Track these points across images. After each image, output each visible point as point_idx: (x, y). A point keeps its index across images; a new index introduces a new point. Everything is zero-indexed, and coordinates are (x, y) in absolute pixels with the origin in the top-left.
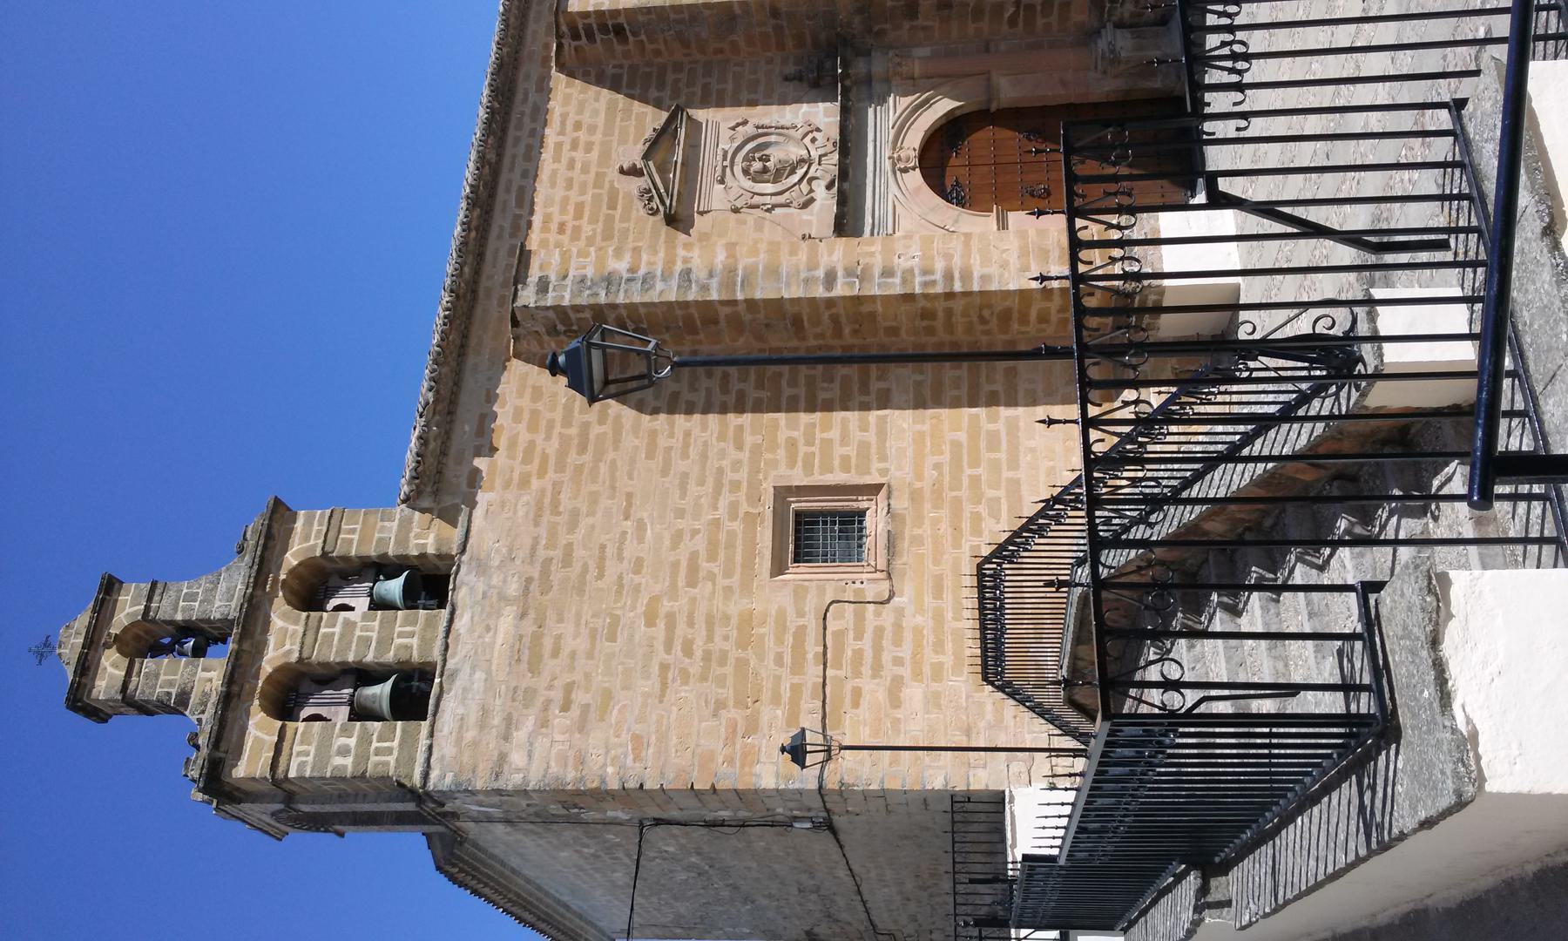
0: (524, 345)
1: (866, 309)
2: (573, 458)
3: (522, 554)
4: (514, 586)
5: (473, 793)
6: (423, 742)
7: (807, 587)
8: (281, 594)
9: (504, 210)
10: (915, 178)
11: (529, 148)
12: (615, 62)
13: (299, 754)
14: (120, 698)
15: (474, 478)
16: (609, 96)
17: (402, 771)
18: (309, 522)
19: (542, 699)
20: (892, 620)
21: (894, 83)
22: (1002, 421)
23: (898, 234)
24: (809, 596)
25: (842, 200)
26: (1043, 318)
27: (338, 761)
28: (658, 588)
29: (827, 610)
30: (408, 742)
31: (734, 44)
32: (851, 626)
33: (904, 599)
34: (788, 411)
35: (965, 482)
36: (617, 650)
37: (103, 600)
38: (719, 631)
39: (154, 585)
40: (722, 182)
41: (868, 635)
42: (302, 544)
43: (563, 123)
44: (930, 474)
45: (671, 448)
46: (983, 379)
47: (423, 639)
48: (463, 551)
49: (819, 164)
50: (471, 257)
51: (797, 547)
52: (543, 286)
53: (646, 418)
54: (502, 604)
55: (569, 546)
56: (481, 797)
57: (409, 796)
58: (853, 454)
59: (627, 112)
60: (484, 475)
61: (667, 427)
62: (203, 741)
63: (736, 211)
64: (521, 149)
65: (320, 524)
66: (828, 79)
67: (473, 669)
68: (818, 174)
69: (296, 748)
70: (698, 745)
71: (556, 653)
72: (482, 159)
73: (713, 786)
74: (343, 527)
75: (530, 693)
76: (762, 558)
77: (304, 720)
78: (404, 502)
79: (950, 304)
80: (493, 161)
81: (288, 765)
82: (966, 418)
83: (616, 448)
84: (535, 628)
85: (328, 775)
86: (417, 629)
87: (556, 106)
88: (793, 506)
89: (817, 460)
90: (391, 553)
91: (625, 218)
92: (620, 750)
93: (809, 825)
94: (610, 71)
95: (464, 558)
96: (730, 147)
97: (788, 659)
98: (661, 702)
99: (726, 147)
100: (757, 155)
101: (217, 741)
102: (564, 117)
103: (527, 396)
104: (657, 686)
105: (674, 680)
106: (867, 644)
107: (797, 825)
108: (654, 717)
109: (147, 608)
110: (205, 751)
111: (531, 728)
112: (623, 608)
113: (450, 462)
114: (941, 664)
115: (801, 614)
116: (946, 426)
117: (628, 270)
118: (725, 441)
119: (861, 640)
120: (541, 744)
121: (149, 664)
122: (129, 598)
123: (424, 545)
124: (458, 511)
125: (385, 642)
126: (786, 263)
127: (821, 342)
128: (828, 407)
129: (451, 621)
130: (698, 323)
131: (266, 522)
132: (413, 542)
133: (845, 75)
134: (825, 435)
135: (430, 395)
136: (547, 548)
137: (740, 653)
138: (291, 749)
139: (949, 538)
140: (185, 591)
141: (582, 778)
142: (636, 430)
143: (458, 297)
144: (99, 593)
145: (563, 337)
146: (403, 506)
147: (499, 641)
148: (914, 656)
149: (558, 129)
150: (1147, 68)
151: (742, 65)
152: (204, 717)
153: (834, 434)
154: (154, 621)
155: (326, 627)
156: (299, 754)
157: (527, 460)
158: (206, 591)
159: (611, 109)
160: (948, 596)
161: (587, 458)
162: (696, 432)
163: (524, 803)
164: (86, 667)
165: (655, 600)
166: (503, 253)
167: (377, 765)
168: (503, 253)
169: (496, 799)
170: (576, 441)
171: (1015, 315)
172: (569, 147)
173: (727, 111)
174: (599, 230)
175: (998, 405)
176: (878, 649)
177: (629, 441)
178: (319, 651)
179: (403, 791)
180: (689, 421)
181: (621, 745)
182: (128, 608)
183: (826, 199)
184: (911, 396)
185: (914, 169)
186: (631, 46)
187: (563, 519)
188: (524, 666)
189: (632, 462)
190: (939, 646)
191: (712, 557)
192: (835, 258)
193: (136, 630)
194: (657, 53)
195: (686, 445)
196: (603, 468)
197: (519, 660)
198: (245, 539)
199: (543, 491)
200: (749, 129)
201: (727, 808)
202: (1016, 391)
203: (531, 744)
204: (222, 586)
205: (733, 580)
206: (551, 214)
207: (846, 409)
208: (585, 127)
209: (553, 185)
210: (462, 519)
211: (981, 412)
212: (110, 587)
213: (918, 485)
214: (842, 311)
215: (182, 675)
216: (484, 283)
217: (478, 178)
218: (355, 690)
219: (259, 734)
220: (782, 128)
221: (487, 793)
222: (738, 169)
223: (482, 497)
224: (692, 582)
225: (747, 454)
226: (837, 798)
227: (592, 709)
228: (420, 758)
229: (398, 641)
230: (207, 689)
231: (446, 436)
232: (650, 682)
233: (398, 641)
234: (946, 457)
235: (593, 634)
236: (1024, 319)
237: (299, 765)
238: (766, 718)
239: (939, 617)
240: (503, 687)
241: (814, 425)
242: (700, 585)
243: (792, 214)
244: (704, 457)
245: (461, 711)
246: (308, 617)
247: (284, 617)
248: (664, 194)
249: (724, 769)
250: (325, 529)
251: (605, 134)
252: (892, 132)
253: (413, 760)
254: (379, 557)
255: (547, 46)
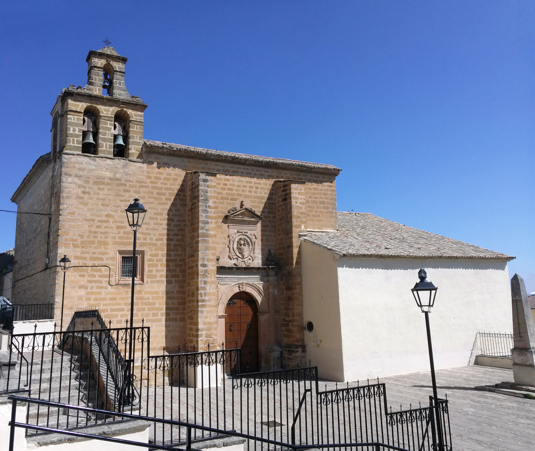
0: (189, 175)
1: (195, 276)
2: (155, 191)
3: (128, 178)
4: (119, 176)
5: (61, 167)
6: (75, 153)
7: (114, 261)
8: (120, 109)
9: (231, 167)
10: (237, 290)
11: (251, 174)
12: (277, 198)
13: (74, 118)
14: (92, 66)
15: (150, 163)
16: (266, 197)
17: (68, 147)
18: (140, 116)
19: (86, 185)
20: (104, 286)
21: (267, 283)
22: (161, 317)
23: (219, 285)
24: (112, 261)
25: (230, 268)
26: (191, 329)
27: (72, 129)
28: (116, 217)
29: (107, 267)
30: (76, 148)
31: (280, 235)
32: (103, 274)
33: (110, 289)
34: (167, 254)
35: (143, 307)
36: (99, 206)
37: (120, 59)
38: (103, 236)
39: (124, 73)
40: (238, 232)
41: (100, 279)
42: (133, 114)
43: (258, 183)
44: (146, 296)
45: (157, 219)
46: (174, 311)
47: (105, 151)
48: (130, 161)
49: (242, 261)
50: (217, 158)
51: (127, 257)
52: (205, 181)
53: (167, 212)
54: (114, 173)
55: (129, 191)
56: (60, 170)
57: (61, 149)
58: (153, 273)
59: (261, 203)
60: (152, 166)
61: (163, 218)
62: (79, 90)
63: (229, 236)
64: (250, 171)
65: (139, 119)
66: (269, 263)
67: (95, 166)
68: (239, 261)
69: (76, 117)
70: (71, 231)
71: (99, 189)
72: (246, 160)
73: (59, 235)
74: (138, 126)
75: (87, 182)
76: (123, 247)
77: (84, 118)
78: (145, 142)
79: (195, 302)
80: (246, 163)
81: (71, 115)
82: (162, 307)
83: (158, 204)
84: (106, 182)
85: (68, 126)
86: (108, 149)
87: (263, 181)
88: (139, 256)
89: (152, 263)
90: (130, 140)
91: (227, 203)
92: (71, 209)
93: (47, 262)
94: (274, 197)
95: (128, 161)
96: (248, 234)
97: (94, 256)
98: (84, 220)
99: (248, 233)
100: (245, 242)
101: (79, 94)
102: (260, 184)
103: (174, 177)
104: (88, 218)
105: (90, 223)
106: (97, 278)
107: (47, 259)
108: (79, 218)
109: (117, 71)
110: (76, 91)
111: (78, 183)
112: (111, 208)
113: (156, 156)
114: (90, 300)
115: (107, 259)
116: (160, 301)
117: (209, 205)
118: (159, 235)
119: (99, 277)
120: (73, 186)
121: (101, 73)
122: (120, 66)
123: (132, 150)
124: (141, 159)
125: (104, 140)
126: (209, 252)
127: (187, 263)
128: (168, 266)
129: (110, 158)
130: (193, 227)
131: (140, 104)
132: (133, 146)
133: (269, 269)
134: (159, 265)
135: (175, 149)
136: (130, 185)
137: (96, 242)
138: (76, 115)
139: (127, 302)
140: (122, 82)
141: (63, 198)
142: (163, 209)
143: (205, 155)
144: (122, 57)
145: (191, 186)
146: (143, 143)
147: (103, 173)
148: (93, 292)
149: (256, 182)
150: (268, 362)
151: (274, 237)
152: (86, 90)
153: (159, 268)
154: (114, 73)
155: (110, 123)
156: (74, 118)
157: (156, 178)
158: (121, 88)
159: (262, 198)
160: (110, 302)
161: (155, 195)
162: (162, 227)
163: (57, 181)
164: (101, 55)
165: (113, 217)
166: (218, 167)
167: (70, 140)
168: (218, 167)
169: (59, 174)
170: (160, 192)
171: (192, 321)
172: (250, 185)
173: (260, 233)
174: (224, 196)
175: (166, 316)
176: (96, 282)
177: (160, 207)
178: (103, 121)
179: (62, 148)
180: (165, 225)
181: (72, 209)
182: (117, 66)
183: (231, 263)
184: (170, 290)
185: (240, 290)
186: (281, 203)
187: (137, 189)
188: (96, 180)
189: (154, 208)
190: (96, 299)
191: (125, 233)
192: (210, 267)
193: (111, 68)
194: (279, 211)
195: (158, 224)
196: (152, 200)
197: (97, 178)
198: (136, 98)
199: (146, 183)
200: (254, 240)
201: (53, 239)
202: (170, 321)
203: (73, 183)
204: (123, 92)
205: (117, 239)
206: (230, 181)
207: (167, 271)
208: (256, 190)
209: (239, 181)
210: (139, 160)
211: (164, 311)
212: (124, 60)
213: (143, 293)
214: (195, 269)
215: (98, 83)
216: (209, 162)
217: (241, 159)
218: (92, 132)
219: (80, 106)
220: (254, 250)
221: (61, 171)
222: (241, 237)
223: (145, 165)
224: (117, 227)
225: (154, 242)
226: (54, 271)
227: (83, 200)
228: (71, 152)
229: (104, 144)
230: (94, 90)
231: (163, 154)
232: (89, 216)
233: (104, 144)
234: (151, 301)
235: (104, 199)
236: (191, 323)
237: (71, 118)
238: (77, 250)
239: (104, 299)
240: (90, 174)
241: (162, 261)
242: (117, 229)
243: (227, 253)
244: (154, 229)
245: (84, 163)
246: (113, 117)
247: (113, 110)
248: (234, 215)
249: (64, 238)
250: (138, 120)
251: (254, 196)
252: (251, 283)
253: (71, 150)
254: (129, 137)
255: (282, 178)
